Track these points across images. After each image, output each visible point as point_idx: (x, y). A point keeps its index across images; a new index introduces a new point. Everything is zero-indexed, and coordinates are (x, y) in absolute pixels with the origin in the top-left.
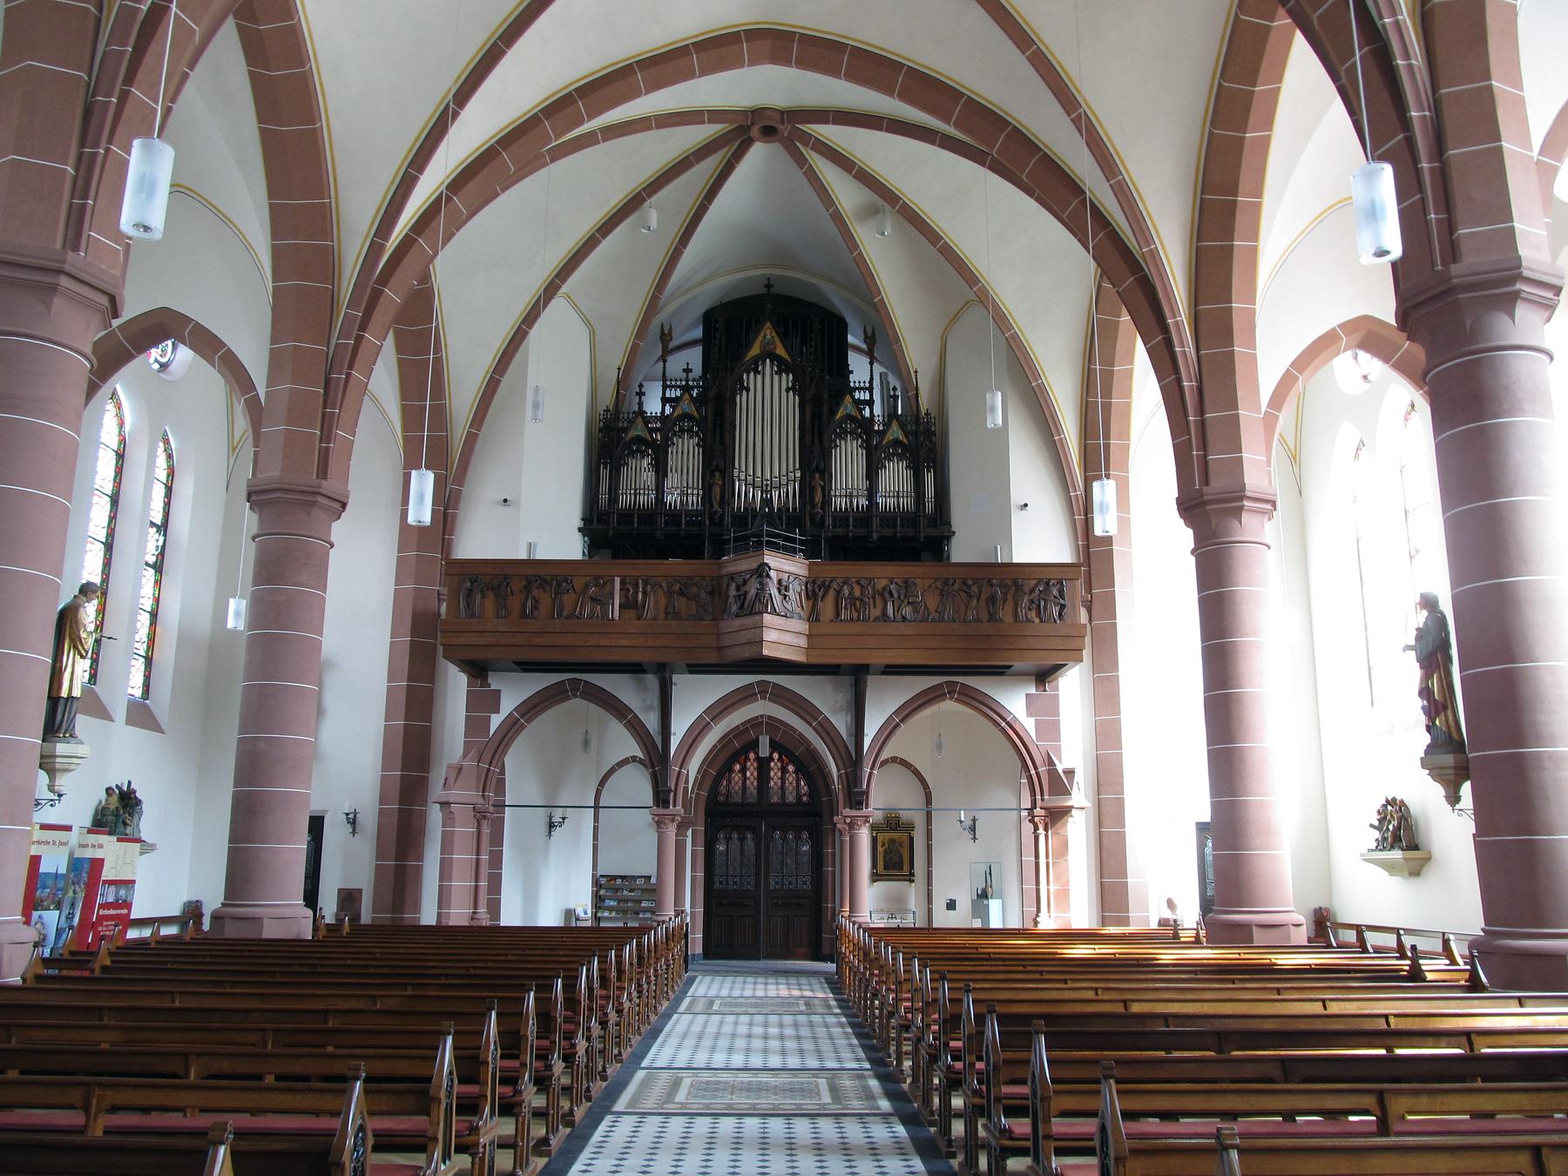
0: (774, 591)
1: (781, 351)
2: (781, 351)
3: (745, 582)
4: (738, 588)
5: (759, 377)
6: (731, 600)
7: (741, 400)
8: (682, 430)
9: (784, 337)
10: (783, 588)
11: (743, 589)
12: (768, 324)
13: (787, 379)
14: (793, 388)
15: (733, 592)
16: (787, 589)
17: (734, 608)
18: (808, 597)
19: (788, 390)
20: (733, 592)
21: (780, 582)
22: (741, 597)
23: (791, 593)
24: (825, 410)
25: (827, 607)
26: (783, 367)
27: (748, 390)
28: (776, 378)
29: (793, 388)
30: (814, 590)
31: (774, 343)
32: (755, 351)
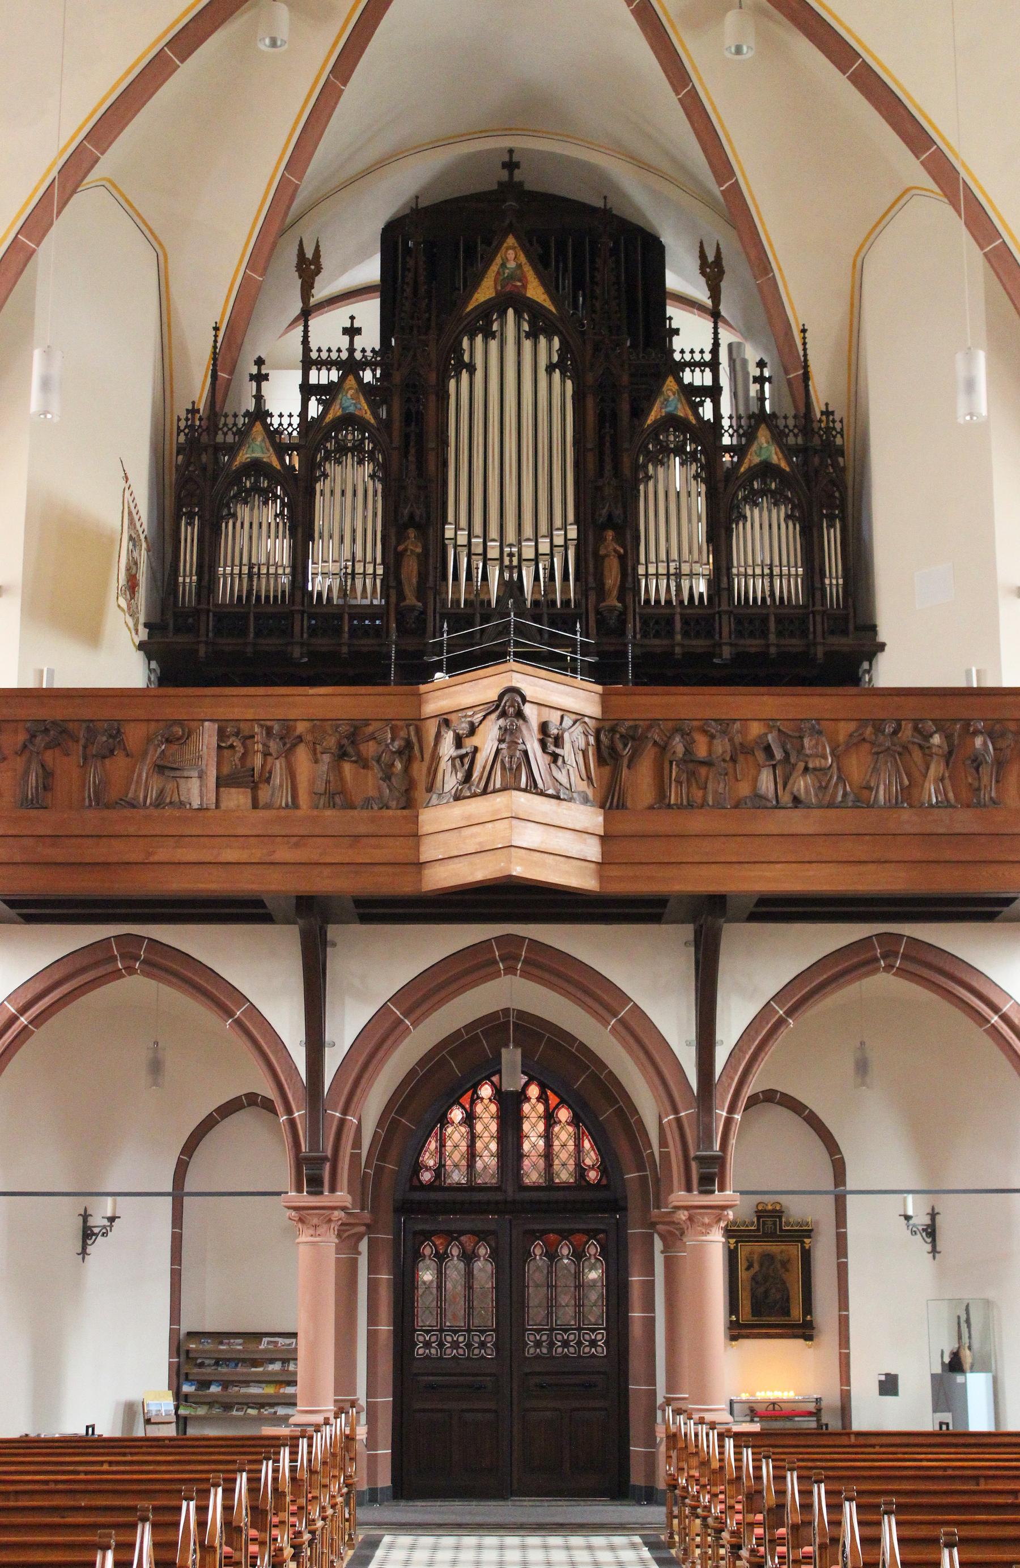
0: (533, 746)
1: (536, 292)
2: (536, 292)
3: (473, 730)
4: (459, 743)
5: (494, 345)
6: (445, 765)
7: (459, 388)
8: (342, 450)
9: (541, 263)
10: (550, 739)
11: (469, 743)
12: (511, 241)
13: (549, 348)
14: (561, 365)
15: (447, 748)
16: (558, 741)
17: (451, 781)
18: (601, 761)
19: (550, 368)
20: (447, 748)
21: (544, 727)
22: (466, 761)
23: (567, 751)
25: (641, 781)
26: (540, 325)
27: (471, 369)
28: (527, 345)
29: (561, 365)
30: (613, 747)
31: (523, 279)
32: (485, 292)
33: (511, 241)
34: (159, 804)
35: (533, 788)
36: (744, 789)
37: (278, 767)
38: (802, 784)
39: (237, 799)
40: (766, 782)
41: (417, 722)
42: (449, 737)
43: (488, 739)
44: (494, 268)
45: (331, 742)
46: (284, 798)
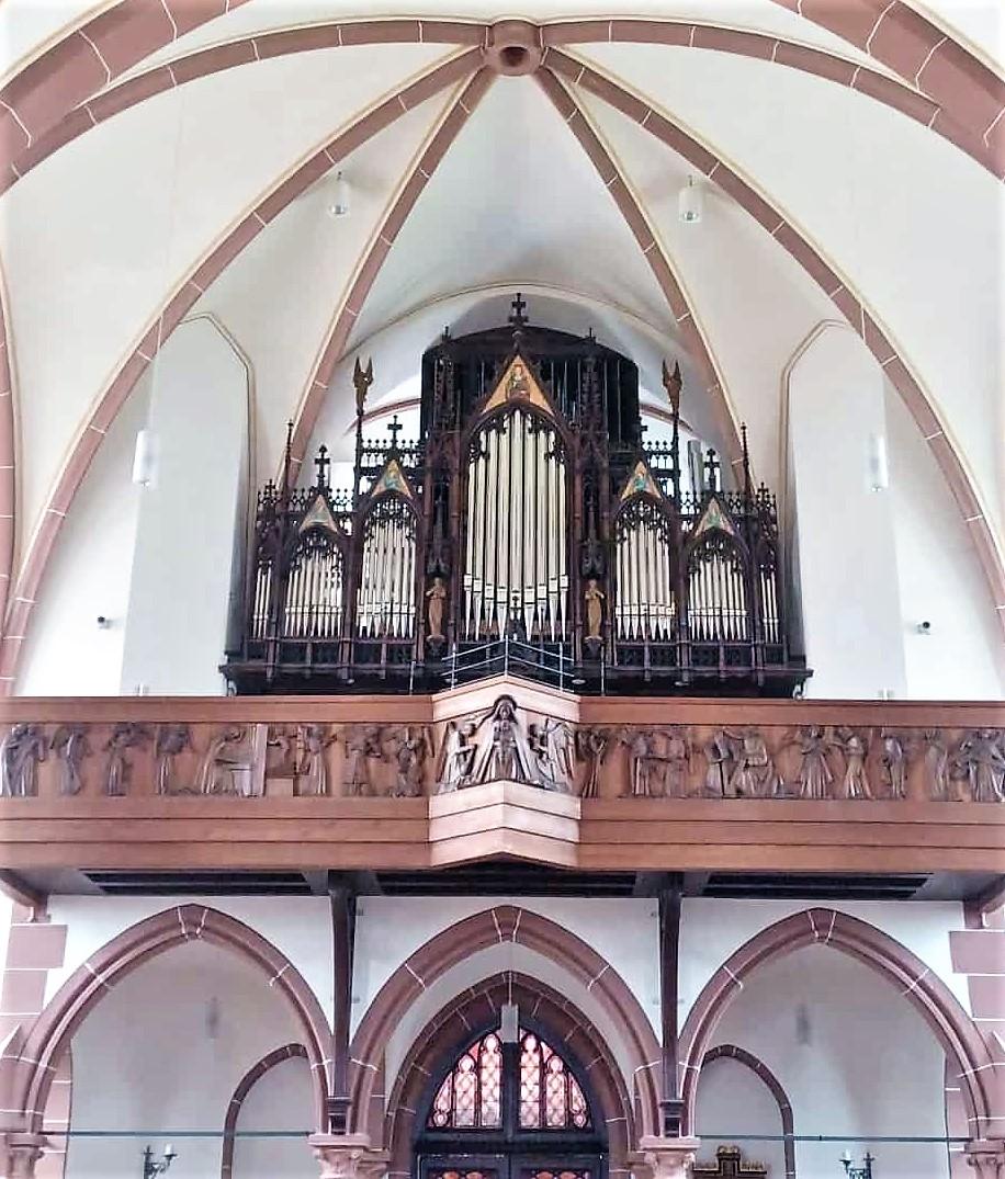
0: (522, 744)
1: (537, 398)
2: (537, 398)
3: (474, 730)
5: (504, 438)
6: (451, 760)
7: (476, 470)
11: (471, 742)
12: (518, 360)
13: (547, 441)
14: (556, 453)
15: (454, 746)
19: (548, 456)
20: (454, 746)
22: (468, 756)
23: (550, 749)
24: (605, 485)
26: (539, 424)
27: (487, 456)
28: (530, 437)
29: (556, 453)
30: (589, 745)
32: (498, 398)
33: (518, 360)
34: (217, 791)
35: (522, 779)
36: (697, 783)
37: (316, 760)
38: (744, 779)
39: (282, 786)
40: (714, 776)
41: (430, 725)
42: (454, 737)
43: (485, 739)
44: (505, 380)
45: (359, 741)
46: (320, 787)
